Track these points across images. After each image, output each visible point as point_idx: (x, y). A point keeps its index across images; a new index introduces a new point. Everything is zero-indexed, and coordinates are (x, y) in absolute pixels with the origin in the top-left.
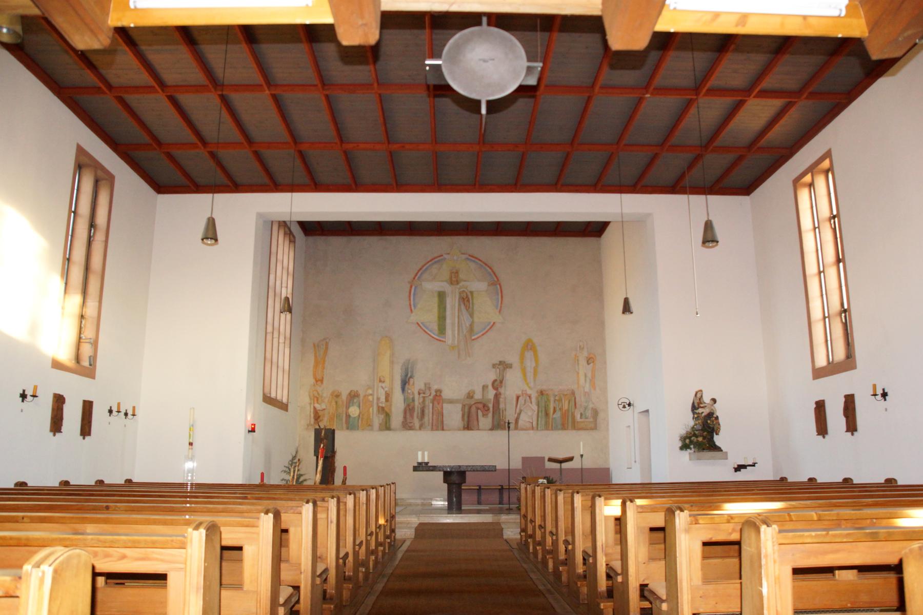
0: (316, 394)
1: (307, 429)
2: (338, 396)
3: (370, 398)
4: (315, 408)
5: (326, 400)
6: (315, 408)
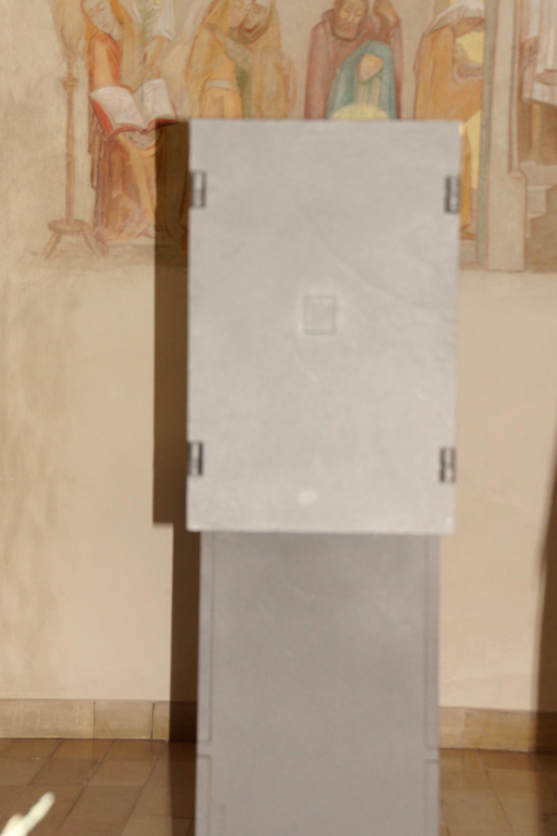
0: (106, 21)
1: (50, 253)
2: (248, 34)
3: (472, 46)
4: (97, 112)
5: (175, 62)
6: (97, 112)
